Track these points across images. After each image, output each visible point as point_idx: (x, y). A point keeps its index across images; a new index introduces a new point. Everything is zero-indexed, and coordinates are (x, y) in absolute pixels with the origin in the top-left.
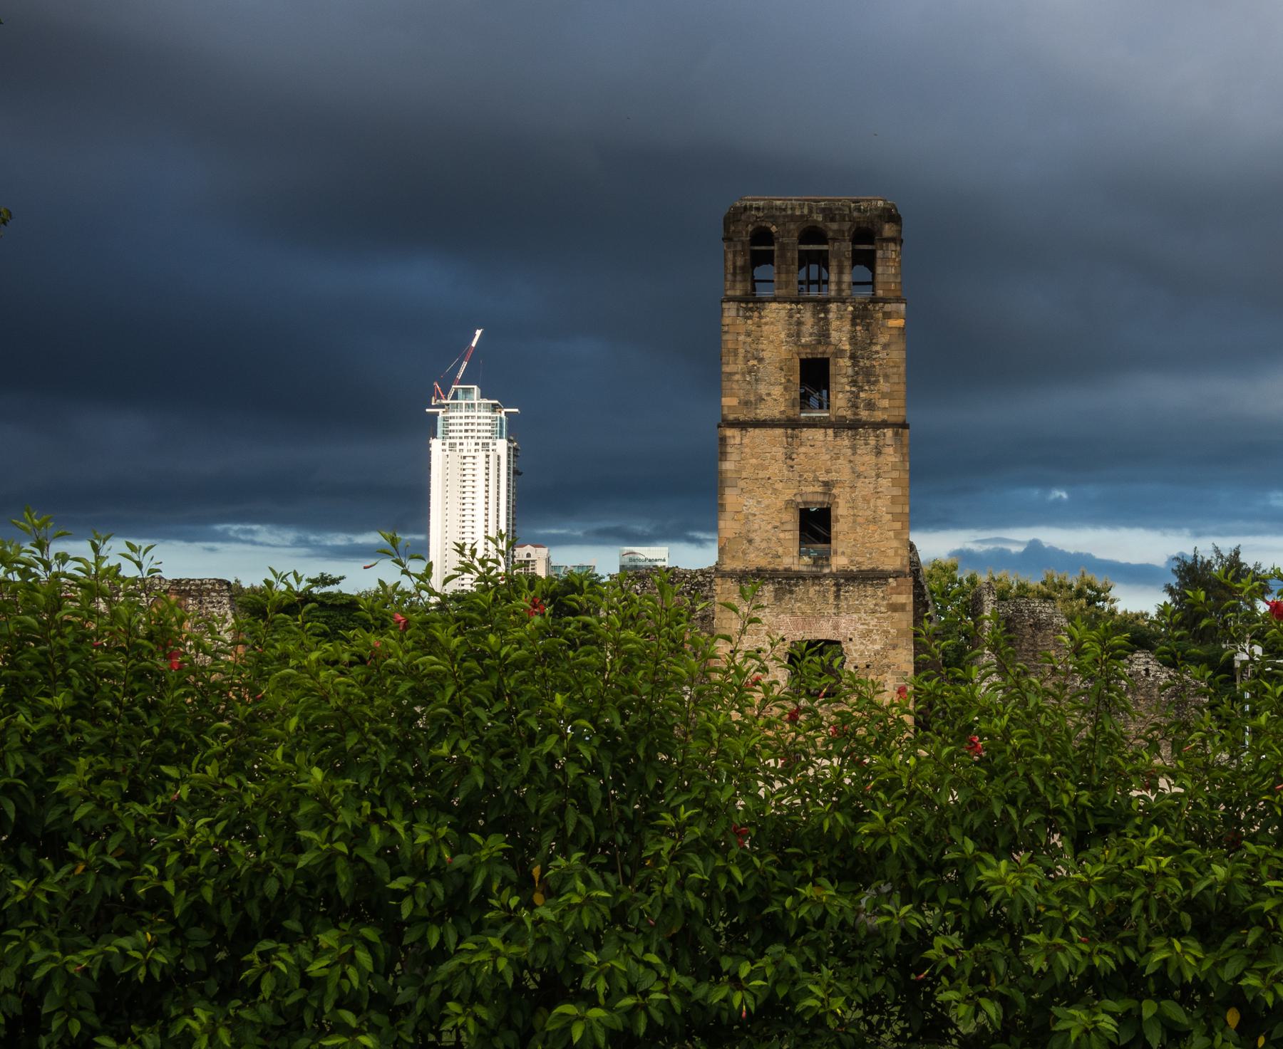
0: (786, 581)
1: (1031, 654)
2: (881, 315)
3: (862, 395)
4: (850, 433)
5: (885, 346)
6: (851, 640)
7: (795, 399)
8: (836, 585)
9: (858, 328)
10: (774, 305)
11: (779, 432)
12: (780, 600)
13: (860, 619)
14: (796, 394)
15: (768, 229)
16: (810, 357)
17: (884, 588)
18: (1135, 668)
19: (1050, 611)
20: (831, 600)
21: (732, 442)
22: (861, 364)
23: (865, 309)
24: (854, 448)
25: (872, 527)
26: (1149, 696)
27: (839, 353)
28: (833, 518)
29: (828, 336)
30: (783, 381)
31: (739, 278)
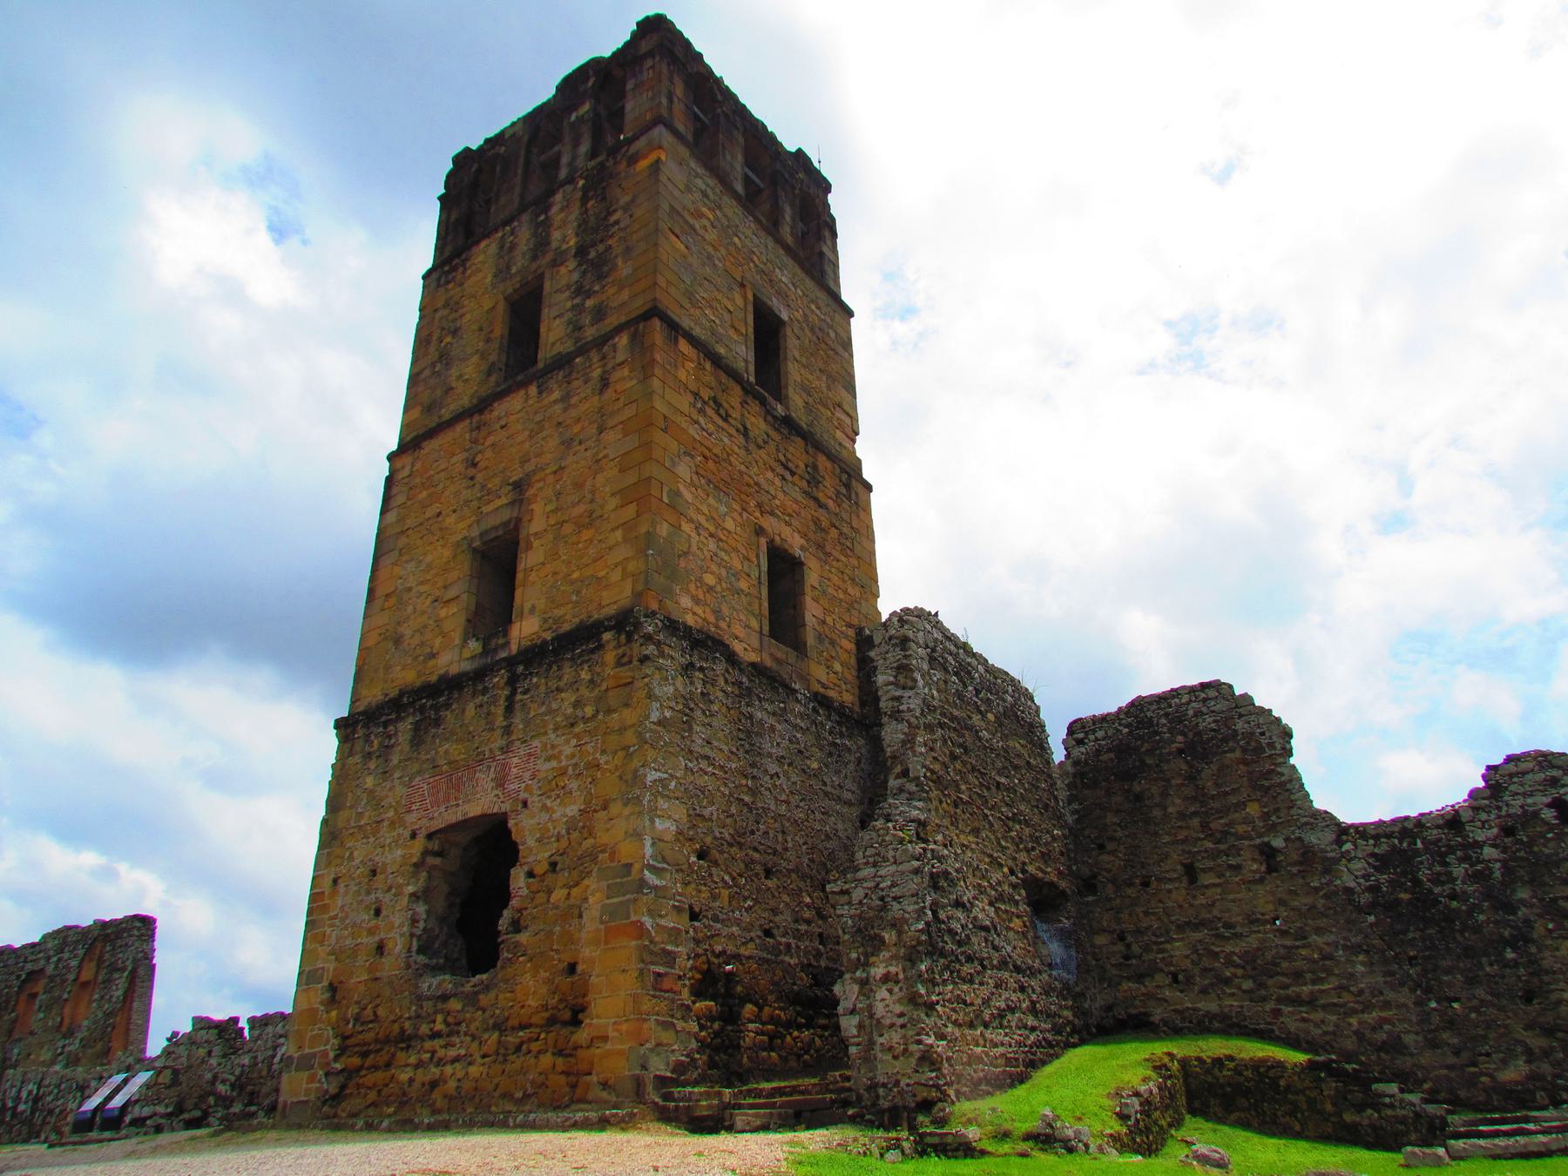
1: (1195, 822)
2: (624, 164)
3: (589, 303)
4: (561, 373)
5: (626, 208)
6: (525, 804)
7: (493, 364)
8: (512, 682)
9: (591, 203)
10: (483, 244)
16: (518, 286)
17: (595, 656)
19: (1221, 706)
20: (500, 721)
22: (593, 254)
28: (522, 545)
30: (481, 344)
31: (450, 238)
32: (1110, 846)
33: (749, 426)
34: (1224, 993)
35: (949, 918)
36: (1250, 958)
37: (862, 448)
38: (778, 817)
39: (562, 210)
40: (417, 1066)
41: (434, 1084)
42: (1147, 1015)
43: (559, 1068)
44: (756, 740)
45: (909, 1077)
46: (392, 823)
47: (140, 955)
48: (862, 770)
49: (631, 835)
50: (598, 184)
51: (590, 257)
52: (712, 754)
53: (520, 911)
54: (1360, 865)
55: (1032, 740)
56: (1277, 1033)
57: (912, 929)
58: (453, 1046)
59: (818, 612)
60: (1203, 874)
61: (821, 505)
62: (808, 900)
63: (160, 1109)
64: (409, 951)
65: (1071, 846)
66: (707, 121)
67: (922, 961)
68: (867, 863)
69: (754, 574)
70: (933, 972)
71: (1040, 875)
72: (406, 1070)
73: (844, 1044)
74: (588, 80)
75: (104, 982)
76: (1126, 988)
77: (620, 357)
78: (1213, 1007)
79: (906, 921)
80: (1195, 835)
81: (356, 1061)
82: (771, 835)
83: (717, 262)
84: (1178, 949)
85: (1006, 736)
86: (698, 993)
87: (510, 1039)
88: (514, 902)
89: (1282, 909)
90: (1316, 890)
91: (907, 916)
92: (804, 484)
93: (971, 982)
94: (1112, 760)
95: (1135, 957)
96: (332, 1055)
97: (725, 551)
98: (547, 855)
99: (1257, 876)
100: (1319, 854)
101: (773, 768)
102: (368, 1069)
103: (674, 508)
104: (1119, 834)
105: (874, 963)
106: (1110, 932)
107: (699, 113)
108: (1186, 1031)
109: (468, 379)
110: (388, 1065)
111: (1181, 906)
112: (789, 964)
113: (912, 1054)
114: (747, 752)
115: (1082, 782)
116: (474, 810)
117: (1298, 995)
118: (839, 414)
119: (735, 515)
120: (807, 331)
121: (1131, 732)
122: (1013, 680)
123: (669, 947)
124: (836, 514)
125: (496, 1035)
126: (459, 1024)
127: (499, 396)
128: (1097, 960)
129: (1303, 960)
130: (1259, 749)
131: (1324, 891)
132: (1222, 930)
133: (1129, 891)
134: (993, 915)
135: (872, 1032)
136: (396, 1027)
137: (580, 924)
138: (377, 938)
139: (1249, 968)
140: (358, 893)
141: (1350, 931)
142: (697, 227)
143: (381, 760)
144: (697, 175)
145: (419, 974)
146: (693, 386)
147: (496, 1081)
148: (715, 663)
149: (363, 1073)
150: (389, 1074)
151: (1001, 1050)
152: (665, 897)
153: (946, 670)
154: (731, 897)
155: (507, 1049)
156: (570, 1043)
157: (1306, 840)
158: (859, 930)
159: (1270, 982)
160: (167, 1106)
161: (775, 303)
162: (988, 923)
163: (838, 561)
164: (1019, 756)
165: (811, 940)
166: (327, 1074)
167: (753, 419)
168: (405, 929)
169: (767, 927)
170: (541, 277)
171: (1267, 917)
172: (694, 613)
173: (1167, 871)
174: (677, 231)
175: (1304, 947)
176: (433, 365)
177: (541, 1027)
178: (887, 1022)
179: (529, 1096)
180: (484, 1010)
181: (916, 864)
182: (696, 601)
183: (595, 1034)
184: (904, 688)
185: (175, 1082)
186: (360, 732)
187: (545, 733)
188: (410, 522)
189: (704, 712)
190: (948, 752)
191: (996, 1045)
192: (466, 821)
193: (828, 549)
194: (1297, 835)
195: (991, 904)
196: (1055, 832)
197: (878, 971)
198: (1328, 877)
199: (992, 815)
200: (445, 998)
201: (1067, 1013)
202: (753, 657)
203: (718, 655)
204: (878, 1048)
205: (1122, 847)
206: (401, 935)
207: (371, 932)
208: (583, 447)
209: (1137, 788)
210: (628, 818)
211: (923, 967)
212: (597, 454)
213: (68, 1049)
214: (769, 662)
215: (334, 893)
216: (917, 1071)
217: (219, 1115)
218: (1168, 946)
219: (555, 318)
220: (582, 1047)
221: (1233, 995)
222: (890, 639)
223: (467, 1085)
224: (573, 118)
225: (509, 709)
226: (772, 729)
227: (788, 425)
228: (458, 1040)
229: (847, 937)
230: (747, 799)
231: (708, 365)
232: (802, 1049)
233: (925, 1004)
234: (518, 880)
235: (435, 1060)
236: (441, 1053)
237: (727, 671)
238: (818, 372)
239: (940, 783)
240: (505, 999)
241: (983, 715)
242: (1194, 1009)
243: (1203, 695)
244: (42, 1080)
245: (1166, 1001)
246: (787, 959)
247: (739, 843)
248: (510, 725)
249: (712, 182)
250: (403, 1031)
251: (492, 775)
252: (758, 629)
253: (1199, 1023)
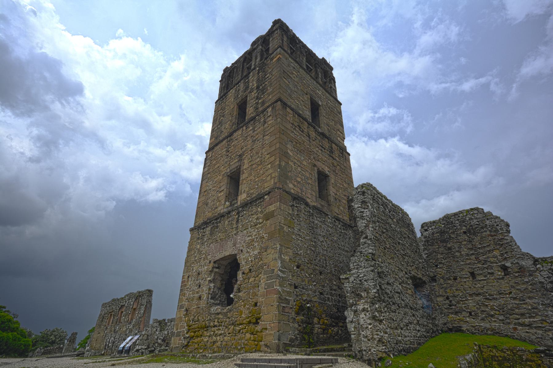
3: (260, 101)
6: (242, 251)
8: (238, 213)
13: (247, 232)
20: (235, 226)
22: (261, 87)
28: (241, 173)
31: (222, 91)
32: (441, 266)
33: (310, 134)
34: (491, 320)
35: (385, 288)
36: (501, 308)
37: (347, 143)
38: (323, 255)
39: (252, 77)
40: (209, 337)
41: (214, 342)
42: (460, 327)
43: (252, 339)
44: (315, 230)
45: (375, 348)
46: (204, 260)
47: (148, 301)
48: (351, 241)
49: (274, 260)
50: (262, 67)
51: (260, 88)
52: (301, 234)
53: (240, 285)
54: (545, 273)
55: (409, 230)
56: (516, 337)
57: (372, 291)
58: (220, 330)
59: (335, 191)
60: (478, 276)
61: (334, 159)
62: (335, 283)
63: (143, 347)
64: (208, 298)
65: (426, 266)
66: (295, 49)
67: (377, 304)
68: (354, 268)
69: (313, 179)
70: (381, 308)
71: (416, 275)
72: (207, 337)
73: (348, 334)
75: (139, 308)
76: (451, 317)
77: (269, 114)
78: (488, 326)
79: (370, 289)
80: (473, 262)
81: (193, 334)
82: (322, 261)
83: (298, 87)
84: (471, 303)
85: (400, 227)
86: (298, 313)
87: (237, 328)
88: (238, 282)
89: (513, 289)
90: (527, 282)
91: (370, 287)
92: (328, 152)
93: (395, 312)
94: (438, 236)
95: (453, 305)
96: (186, 332)
97: (304, 171)
98: (248, 267)
99: (501, 277)
100: (527, 269)
101: (322, 239)
102: (196, 337)
103: (286, 157)
104: (443, 261)
105: (358, 304)
106: (442, 296)
107: (292, 47)
108: (477, 334)
109: (227, 127)
110: (201, 336)
111: (470, 287)
112: (329, 304)
113: (375, 339)
114: (312, 234)
115: (428, 243)
116: (227, 254)
117: (524, 323)
118: (338, 133)
119: (307, 160)
120: (328, 108)
121: (445, 226)
122: (401, 209)
123: (287, 298)
124: (339, 162)
125: (232, 327)
126: (222, 322)
127: (235, 131)
128: (439, 306)
129: (524, 309)
130: (497, 231)
131: (531, 283)
132: (488, 296)
133: (449, 282)
134: (401, 288)
135: (359, 330)
136: (204, 323)
137: (258, 289)
138: (199, 294)
139: (501, 311)
140: (194, 280)
141: (544, 298)
142: (292, 77)
143: (202, 240)
144: (292, 63)
145: (211, 306)
146: (291, 122)
147: (233, 342)
148: (301, 205)
149: (194, 338)
150: (201, 339)
151: (408, 338)
152: (286, 280)
153: (378, 203)
154: (309, 282)
155: (236, 331)
156: (256, 330)
157: (520, 264)
158: (353, 292)
159: (511, 317)
160: (145, 346)
161: (317, 99)
162: (399, 291)
163: (340, 176)
164: (405, 234)
165: (336, 297)
166: (184, 338)
167: (311, 132)
168: (207, 291)
169: (321, 291)
170: (247, 96)
171: (507, 292)
172: (294, 190)
173: (464, 275)
174: (286, 78)
175: (524, 304)
176: (218, 126)
177: (246, 324)
178: (365, 326)
179: (242, 348)
180: (229, 318)
181: (372, 268)
182: (295, 186)
183: (263, 327)
184: (364, 209)
185: (147, 339)
187: (248, 228)
188: (211, 170)
189: (297, 220)
190: (381, 231)
191: (406, 337)
192: (225, 257)
193: (337, 172)
194: (516, 262)
195: (400, 284)
196: (420, 260)
197: (360, 307)
198: (532, 278)
199: (398, 253)
200: (218, 314)
201: (430, 325)
202: (314, 204)
203: (302, 202)
204: (362, 336)
205: (445, 266)
206: (206, 293)
207: (197, 293)
208: (259, 142)
209: (449, 246)
210: (273, 254)
211: (377, 306)
212: (263, 143)
213: (130, 327)
214: (319, 206)
215: (188, 281)
216: (377, 346)
217: (158, 349)
218: (466, 302)
219: (250, 107)
220: (259, 332)
221: (495, 321)
222: (359, 192)
223: (224, 343)
225: (238, 221)
226: (321, 226)
227: (323, 135)
228: (221, 328)
229: (348, 294)
230: (313, 249)
231: (296, 116)
232: (334, 334)
233: (379, 320)
234: (240, 276)
235: (215, 334)
236: (217, 332)
237: (305, 208)
238: (331, 120)
239: (379, 241)
240: (236, 314)
241: (392, 220)
242: (480, 326)
243: (472, 213)
244: (115, 336)
245: (468, 322)
246: (328, 302)
247: (311, 263)
248: (238, 227)
249: (296, 65)
250: (206, 324)
251: (232, 242)
252: (315, 195)
253: (482, 331)
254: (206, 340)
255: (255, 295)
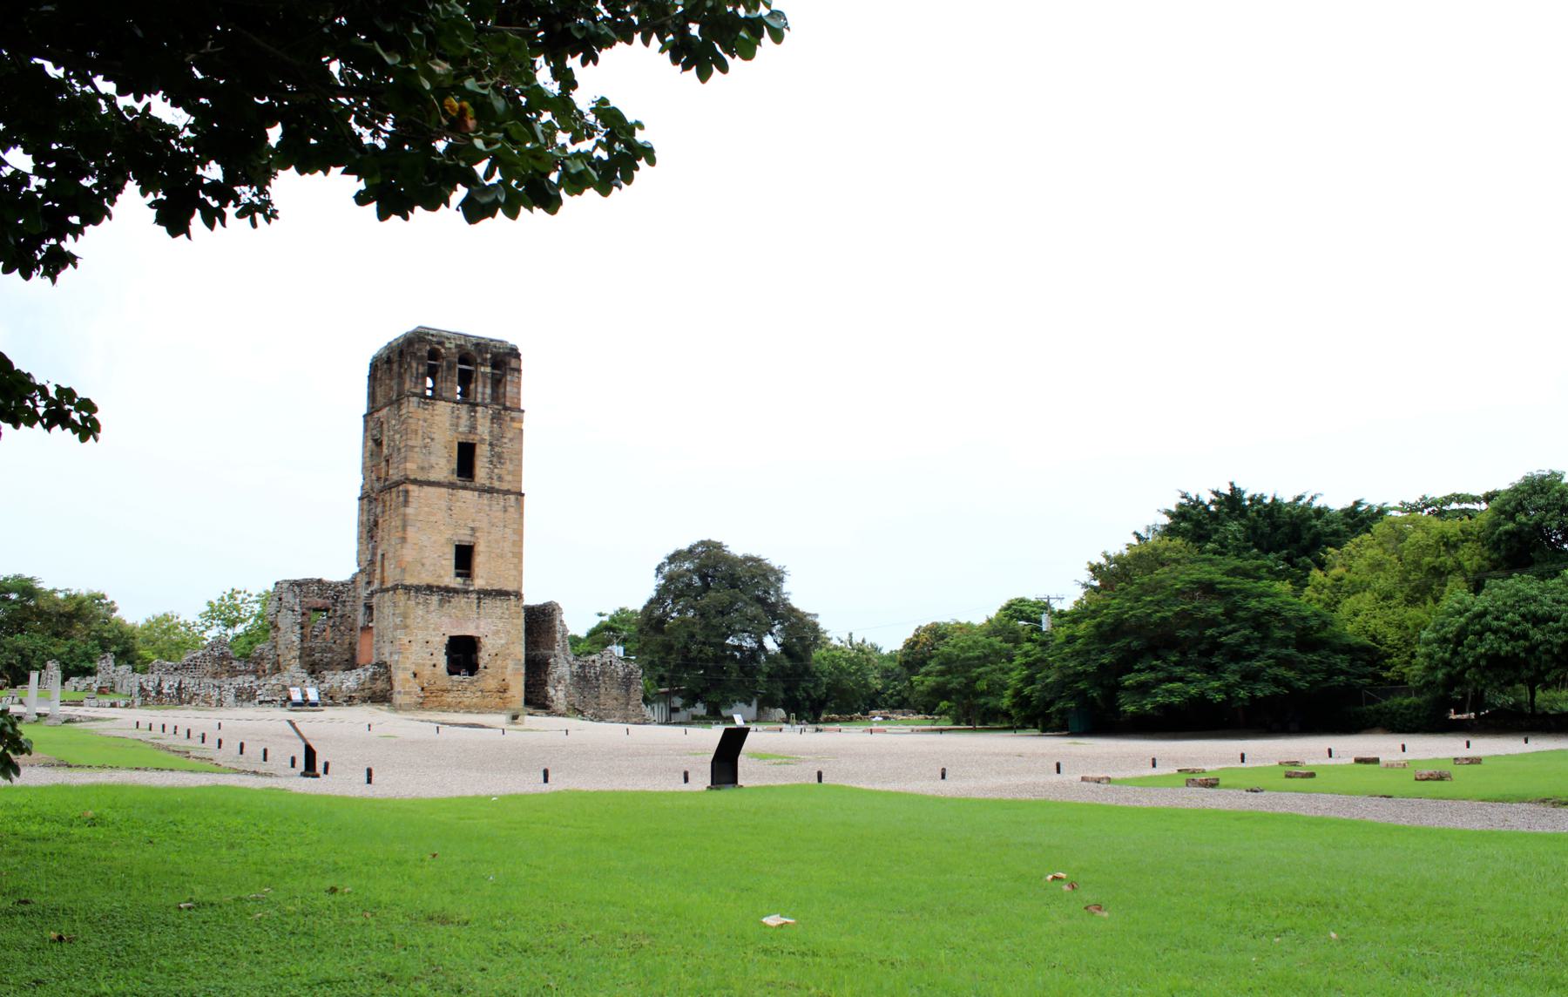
0: (448, 591)
2: (508, 419)
3: (496, 471)
4: (489, 495)
5: (511, 440)
8: (479, 598)
10: (443, 403)
11: (444, 490)
12: (443, 607)
14: (455, 466)
15: (439, 350)
18: (604, 660)
21: (411, 494)
22: (496, 450)
23: (499, 413)
24: (490, 506)
25: (500, 561)
26: (611, 678)
27: (482, 441)
29: (475, 428)
31: (420, 381)
74: (487, 353)
138: (433, 663)
186: (412, 593)
224: (482, 369)
254: (449, 700)
255: (502, 673)
